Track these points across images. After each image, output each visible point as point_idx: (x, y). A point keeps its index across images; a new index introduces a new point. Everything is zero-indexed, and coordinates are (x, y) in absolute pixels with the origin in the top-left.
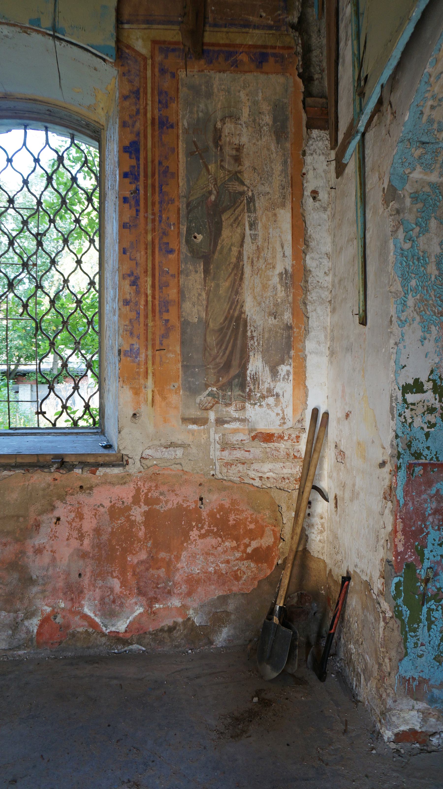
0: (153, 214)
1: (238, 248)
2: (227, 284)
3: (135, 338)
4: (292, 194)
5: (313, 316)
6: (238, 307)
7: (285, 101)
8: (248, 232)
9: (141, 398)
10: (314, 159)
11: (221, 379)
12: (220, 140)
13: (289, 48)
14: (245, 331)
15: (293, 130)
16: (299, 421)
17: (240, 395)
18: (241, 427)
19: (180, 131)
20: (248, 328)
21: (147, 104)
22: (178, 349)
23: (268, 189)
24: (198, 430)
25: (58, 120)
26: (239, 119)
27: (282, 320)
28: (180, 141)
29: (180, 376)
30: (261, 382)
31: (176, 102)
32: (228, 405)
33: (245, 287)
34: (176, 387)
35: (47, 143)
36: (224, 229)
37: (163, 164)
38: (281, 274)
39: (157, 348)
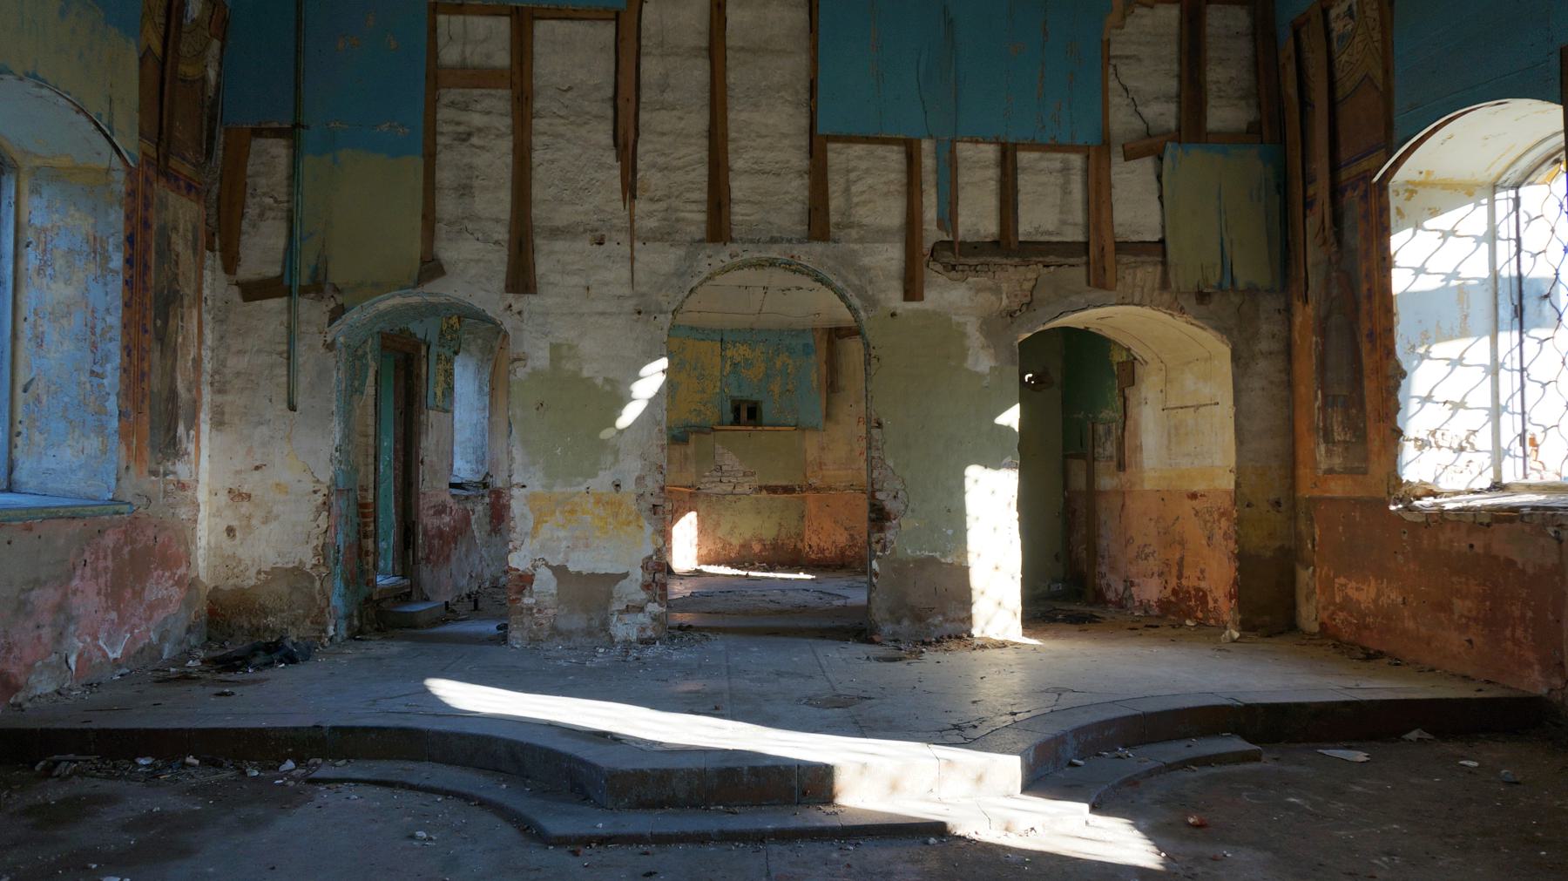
8: (180, 323)
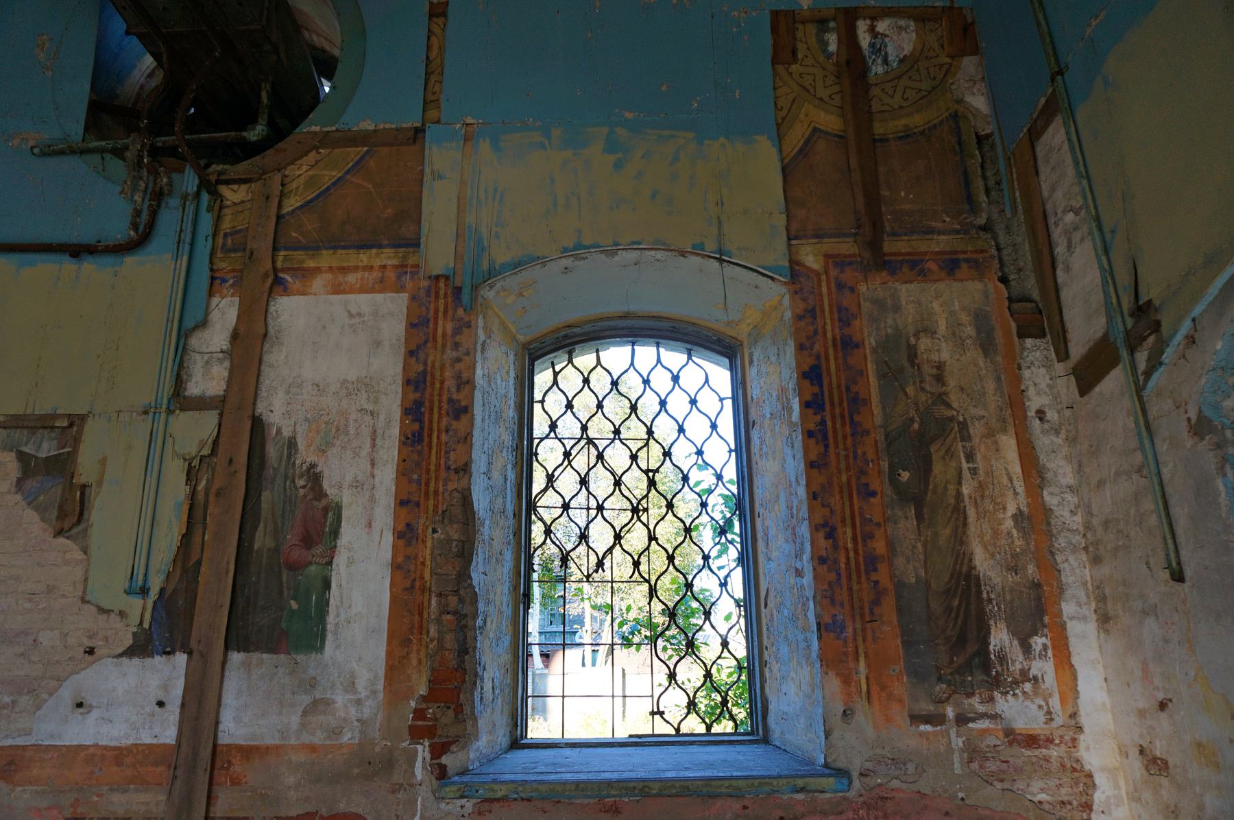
0: (846, 449)
2: (948, 531)
4: (1013, 416)
5: (1064, 566)
6: (966, 561)
7: (988, 309)
8: (965, 465)
9: (853, 689)
10: (1032, 373)
12: (917, 358)
13: (982, 251)
14: (979, 592)
16: (1071, 716)
17: (984, 681)
18: (992, 726)
19: (868, 351)
20: (983, 587)
21: (825, 323)
22: (894, 618)
23: (982, 413)
25: (681, 336)
26: (935, 332)
28: (869, 362)
30: (1010, 662)
32: (970, 695)
33: (971, 534)
34: (897, 671)
35: (659, 361)
38: (1014, 517)
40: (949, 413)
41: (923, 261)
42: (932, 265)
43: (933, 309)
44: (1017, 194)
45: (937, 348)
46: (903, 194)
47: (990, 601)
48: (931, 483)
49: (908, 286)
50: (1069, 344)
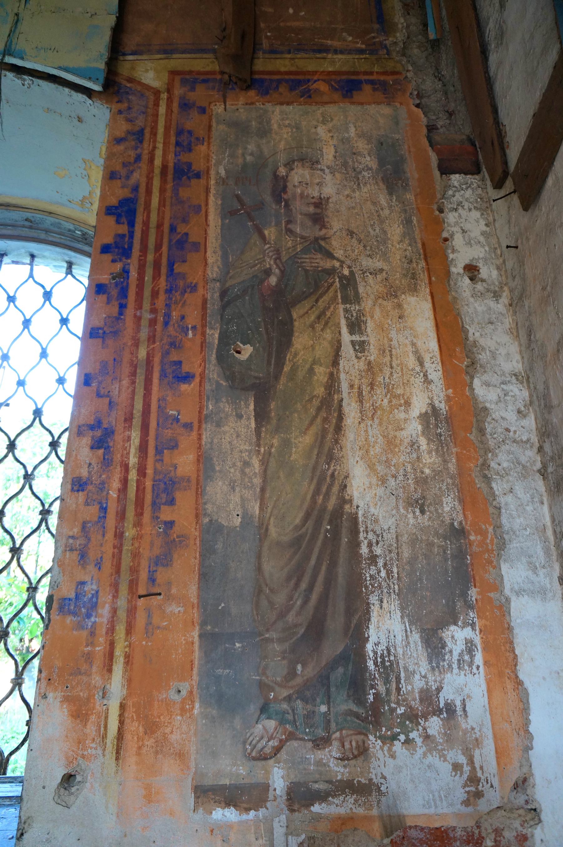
0: (153, 310)
1: (327, 367)
2: (308, 439)
3: (91, 568)
4: (428, 270)
6: (335, 489)
7: (397, 136)
8: (346, 337)
9: (91, 729)
10: (460, 216)
11: (299, 667)
12: (285, 192)
14: (355, 544)
15: (416, 176)
16: (516, 787)
18: (360, 811)
19: (212, 182)
20: (362, 536)
21: (155, 148)
22: (193, 591)
23: (379, 264)
24: (241, 823)
25: (43, 236)
26: (318, 162)
27: (439, 515)
28: (211, 195)
29: (196, 662)
30: (403, 675)
31: (205, 144)
33: (349, 446)
35: (31, 276)
36: (296, 334)
37: (179, 230)
38: (424, 418)
39: (142, 591)
40: (328, 264)
41: (309, 81)
42: (323, 87)
43: (317, 134)
44: (444, 13)
45: (317, 181)
46: (291, 11)
47: (373, 559)
48: (287, 362)
49: (284, 107)
50: (508, 151)
